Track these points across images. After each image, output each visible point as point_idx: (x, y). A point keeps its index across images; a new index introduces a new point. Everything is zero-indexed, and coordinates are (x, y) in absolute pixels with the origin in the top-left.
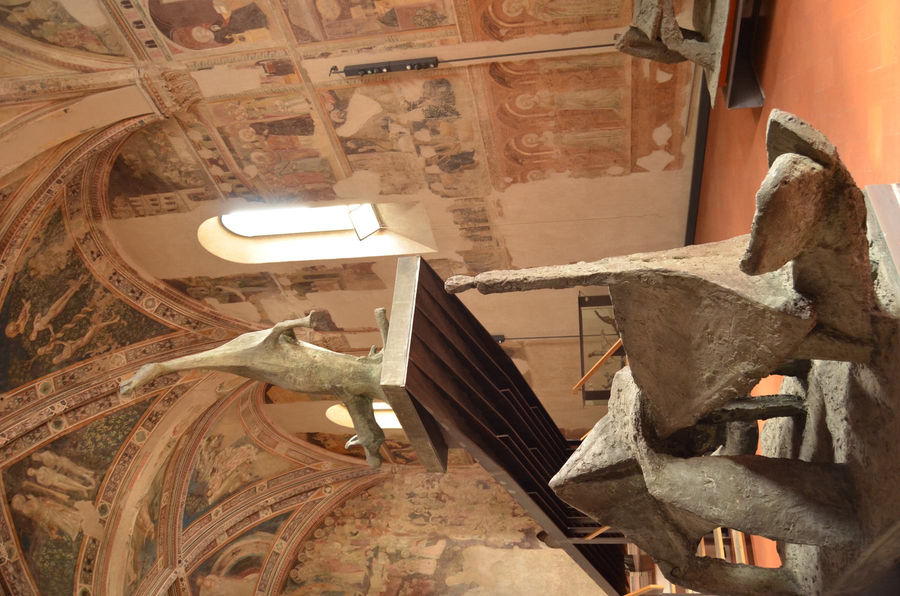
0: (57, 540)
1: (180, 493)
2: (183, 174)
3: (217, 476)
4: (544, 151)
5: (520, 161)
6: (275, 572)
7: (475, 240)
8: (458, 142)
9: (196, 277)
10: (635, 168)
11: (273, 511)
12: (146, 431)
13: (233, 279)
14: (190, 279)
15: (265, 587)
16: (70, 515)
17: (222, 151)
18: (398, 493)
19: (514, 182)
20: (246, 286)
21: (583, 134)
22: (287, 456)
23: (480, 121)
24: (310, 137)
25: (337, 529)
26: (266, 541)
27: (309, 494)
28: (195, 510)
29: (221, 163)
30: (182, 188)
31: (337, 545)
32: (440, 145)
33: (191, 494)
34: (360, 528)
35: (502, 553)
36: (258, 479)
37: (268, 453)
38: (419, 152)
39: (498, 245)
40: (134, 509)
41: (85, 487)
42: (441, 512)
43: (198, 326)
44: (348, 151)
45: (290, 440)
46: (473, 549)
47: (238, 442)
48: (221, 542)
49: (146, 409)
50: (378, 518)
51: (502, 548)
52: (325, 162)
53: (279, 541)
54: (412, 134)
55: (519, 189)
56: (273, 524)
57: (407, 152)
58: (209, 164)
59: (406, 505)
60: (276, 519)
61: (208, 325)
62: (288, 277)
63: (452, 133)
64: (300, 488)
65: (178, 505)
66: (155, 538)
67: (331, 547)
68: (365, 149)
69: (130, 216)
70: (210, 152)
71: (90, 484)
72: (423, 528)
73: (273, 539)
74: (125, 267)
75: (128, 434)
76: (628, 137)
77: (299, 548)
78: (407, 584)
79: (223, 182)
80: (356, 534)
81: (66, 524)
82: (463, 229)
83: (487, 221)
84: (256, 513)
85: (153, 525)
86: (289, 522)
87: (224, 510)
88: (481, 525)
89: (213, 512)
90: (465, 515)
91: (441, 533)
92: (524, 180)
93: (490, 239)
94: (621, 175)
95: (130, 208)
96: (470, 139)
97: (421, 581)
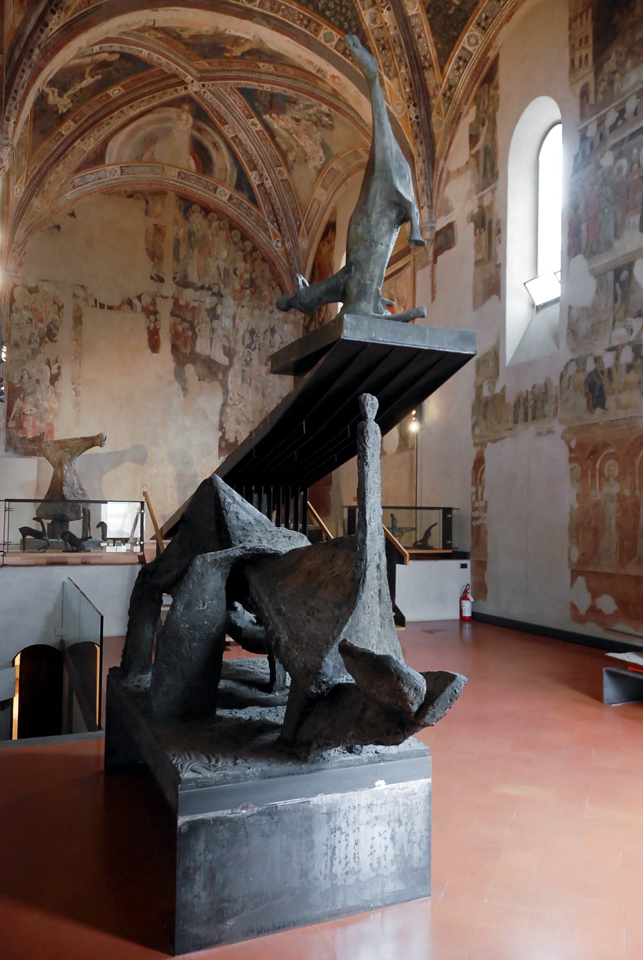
1: (272, 84)
2: (612, 77)
3: (292, 124)
4: (600, 481)
5: (591, 457)
6: (197, 189)
7: (515, 406)
8: (617, 392)
9: (498, 96)
10: (575, 574)
11: (258, 186)
12: (334, 43)
13: (493, 140)
14: (496, 88)
15: (183, 179)
17: (632, 125)
18: (275, 317)
19: (571, 450)
20: (486, 155)
21: (613, 524)
22: (314, 200)
23: (636, 417)
24: (638, 228)
25: (240, 255)
26: (228, 179)
28: (257, 101)
29: (620, 122)
30: (596, 75)
31: (224, 254)
32: (615, 375)
33: (272, 95)
34: (241, 278)
35: (216, 419)
36: (290, 170)
37: (316, 180)
38: (610, 350)
39: (509, 429)
40: (253, 34)
42: (255, 362)
43: (446, 99)
44: (618, 272)
45: (329, 203)
46: (220, 391)
47: (327, 146)
48: (225, 129)
50: (250, 297)
51: (220, 421)
52: (609, 246)
53: (228, 193)
54: (630, 343)
55: (564, 453)
57: (611, 337)
58: (619, 109)
59: (264, 325)
61: (447, 110)
62: (492, 203)
63: (627, 387)
64: (281, 214)
65: (261, 82)
66: (227, 57)
67: (222, 248)
68: (619, 291)
69: (571, 10)
70: (633, 110)
72: (240, 343)
73: (230, 186)
74: (514, 6)
75: (330, 21)
76: (607, 570)
77: (221, 215)
78: (187, 325)
79: (599, 125)
80: (235, 273)
82: (527, 393)
83: (534, 418)
84: (254, 168)
85: (239, 54)
86: (247, 204)
87: (258, 132)
88: (242, 400)
89: (255, 120)
90: (252, 384)
91: (235, 360)
92: (571, 460)
93: (516, 422)
94: (570, 560)
95: (579, 11)
96: (619, 406)
97: (189, 340)
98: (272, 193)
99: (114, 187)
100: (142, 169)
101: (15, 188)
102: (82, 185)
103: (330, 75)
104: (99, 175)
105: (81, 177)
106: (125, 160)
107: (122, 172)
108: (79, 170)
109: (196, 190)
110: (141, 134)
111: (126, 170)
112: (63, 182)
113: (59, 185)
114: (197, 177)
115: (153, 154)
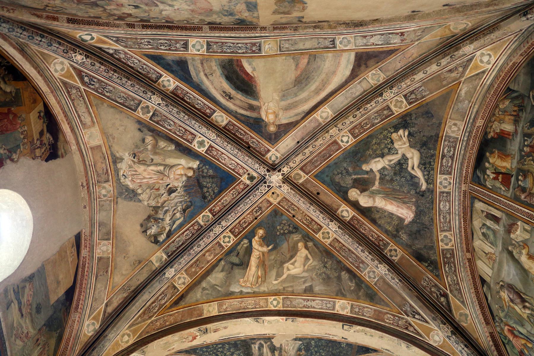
0: (305, 351)
11: (161, 76)
15: (254, 44)
16: (287, 348)
26: (200, 66)
27: (111, 52)
36: (141, 125)
37: (110, 147)
41: (264, 345)
45: (78, 144)
49: (191, 350)
53: (192, 50)
56: (175, 68)
60: (167, 67)
71: (260, 343)
73: (193, 60)
81: (293, 348)
89: (202, 150)
100: (308, 45)
101: (490, 66)
102: (390, 34)
103: (197, 336)
104: (365, 41)
105: (391, 44)
106: (330, 55)
107: (333, 41)
108: (391, 52)
110: (313, 87)
111: (327, 43)
112: (417, 43)
113: (423, 40)
114: (237, 53)
115: (297, 65)
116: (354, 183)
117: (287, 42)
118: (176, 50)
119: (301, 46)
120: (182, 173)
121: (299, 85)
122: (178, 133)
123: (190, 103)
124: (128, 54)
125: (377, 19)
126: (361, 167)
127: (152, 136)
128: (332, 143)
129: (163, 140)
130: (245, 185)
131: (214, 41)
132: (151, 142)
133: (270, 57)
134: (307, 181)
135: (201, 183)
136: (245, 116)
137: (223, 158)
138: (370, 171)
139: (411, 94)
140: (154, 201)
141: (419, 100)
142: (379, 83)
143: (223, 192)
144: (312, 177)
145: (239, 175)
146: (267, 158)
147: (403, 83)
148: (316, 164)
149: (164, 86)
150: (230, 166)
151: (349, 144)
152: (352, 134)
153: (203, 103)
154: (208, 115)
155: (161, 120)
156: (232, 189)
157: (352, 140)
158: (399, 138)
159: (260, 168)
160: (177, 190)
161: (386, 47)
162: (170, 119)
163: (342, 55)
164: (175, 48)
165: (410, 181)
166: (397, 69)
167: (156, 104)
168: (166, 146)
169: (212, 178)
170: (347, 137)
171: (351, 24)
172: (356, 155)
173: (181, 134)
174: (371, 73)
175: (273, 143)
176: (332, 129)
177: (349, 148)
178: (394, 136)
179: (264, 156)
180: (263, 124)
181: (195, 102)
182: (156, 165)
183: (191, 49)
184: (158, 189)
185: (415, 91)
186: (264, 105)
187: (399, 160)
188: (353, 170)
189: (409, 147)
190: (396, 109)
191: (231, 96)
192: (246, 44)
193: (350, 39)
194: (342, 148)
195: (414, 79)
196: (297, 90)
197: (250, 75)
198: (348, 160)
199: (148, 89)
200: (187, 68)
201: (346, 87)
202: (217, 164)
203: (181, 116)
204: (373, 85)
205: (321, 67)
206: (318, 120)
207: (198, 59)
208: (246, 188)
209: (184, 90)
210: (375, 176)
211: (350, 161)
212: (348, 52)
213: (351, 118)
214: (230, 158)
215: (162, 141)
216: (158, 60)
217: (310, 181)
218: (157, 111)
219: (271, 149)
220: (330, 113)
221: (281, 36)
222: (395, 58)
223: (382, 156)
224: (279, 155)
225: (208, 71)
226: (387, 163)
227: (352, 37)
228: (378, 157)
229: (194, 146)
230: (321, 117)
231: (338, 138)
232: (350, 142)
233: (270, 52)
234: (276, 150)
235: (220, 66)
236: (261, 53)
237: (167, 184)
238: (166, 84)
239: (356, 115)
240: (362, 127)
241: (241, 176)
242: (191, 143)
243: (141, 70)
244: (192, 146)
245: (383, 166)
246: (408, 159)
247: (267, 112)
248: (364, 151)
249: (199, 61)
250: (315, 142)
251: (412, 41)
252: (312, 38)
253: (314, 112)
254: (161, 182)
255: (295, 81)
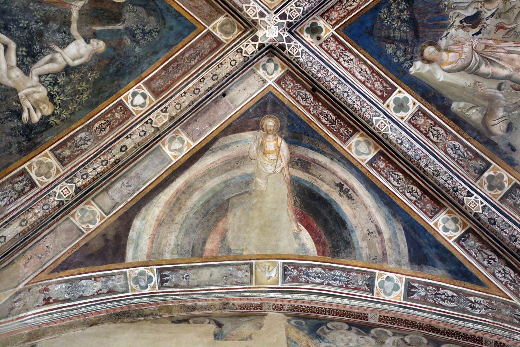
15: (295, 280)
26: (389, 251)
28: (389, 39)
56: (432, 253)
73: (398, 263)
98: (494, 217)
99: (143, 306)
100: (205, 275)
102: (69, 300)
107: (163, 281)
109: (329, 299)
110: (196, 197)
111: (173, 278)
112: (21, 286)
113: (11, 292)
115: (224, 238)
116: (121, 14)
117: (239, 280)
118: (428, 284)
119: (217, 273)
120: (444, 54)
121: (220, 201)
122: (442, 131)
123: (412, 184)
124: (512, 292)
125: (92, 325)
126: (107, 46)
127: (491, 133)
128: (162, 92)
129: (472, 124)
130: (328, 17)
131: (361, 292)
132: (496, 122)
133: (269, 255)
134: (210, 19)
135: (411, 30)
136: (316, 151)
137: (364, 73)
138: (90, 38)
139: (22, 191)
140: (513, 4)
141: (7, 180)
142: (81, 206)
143: (370, 7)
144: (199, 26)
145: (337, 39)
146: (283, 68)
147: (40, 215)
148: (192, 52)
149: (455, 220)
150: (352, 57)
151: (131, 91)
152: (126, 109)
153: (389, 181)
154: (382, 158)
155: (471, 160)
156: (353, 10)
157: (126, 98)
158: (38, 106)
159: (298, 54)
160: (461, 22)
161: (73, 275)
162: (454, 159)
163: (148, 257)
164: (428, 288)
165: (10, 21)
166: (52, 235)
167: (476, 195)
168: (468, 111)
169: (388, 37)
170: (135, 103)
171: (135, 315)
172: (118, 71)
173: (436, 128)
174: (97, 225)
175: (270, 96)
176: (164, 125)
177: (132, 83)
178: (48, 110)
179: (288, 73)
180: (286, 132)
181: (403, 183)
182: (493, 77)
183: (402, 283)
184: (499, 27)
185: (16, 197)
186: (283, 168)
187: (34, 62)
188: (122, 39)
189: (18, 89)
190: (49, 160)
191: (339, 189)
192: (307, 282)
193: (134, 286)
194: (145, 84)
195: (21, 225)
196: (224, 192)
197: (303, 225)
198: (133, 60)
199: (485, 225)
200: (412, 250)
201: (139, 198)
202: (377, 63)
203: (431, 167)
204: (93, 203)
205: (183, 233)
206: (189, 135)
207: (391, 263)
208: (326, 12)
209: (421, 209)
210: (79, 29)
211: (129, 57)
212: (138, 262)
213: (130, 144)
214: (350, 72)
215: (473, 122)
216: (460, 271)
217: (204, 19)
218: (474, 176)
219: (275, 85)
220: (166, 149)
221: (250, 292)
222: (57, 254)
223: (68, 70)
224: (261, 72)
225: (375, 240)
226: (58, 56)
227: (133, 290)
228: (76, 67)
229: (414, 104)
230: (182, 141)
231: (151, 101)
232: (130, 95)
233: (268, 264)
234: (265, 82)
235: (354, 247)
236: (283, 263)
237: (480, 36)
238: (451, 225)
239: (121, 151)
240: (108, 123)
241: (333, 36)
242: (420, 110)
243: (494, 257)
244: (418, 103)
245: (66, 50)
246: (18, 65)
247: (278, 155)
248: (102, 78)
249: (389, 259)
250: (195, 100)
251: (29, 289)
252: (198, 286)
253: (195, 151)
254: (491, 42)
255: (227, 210)
